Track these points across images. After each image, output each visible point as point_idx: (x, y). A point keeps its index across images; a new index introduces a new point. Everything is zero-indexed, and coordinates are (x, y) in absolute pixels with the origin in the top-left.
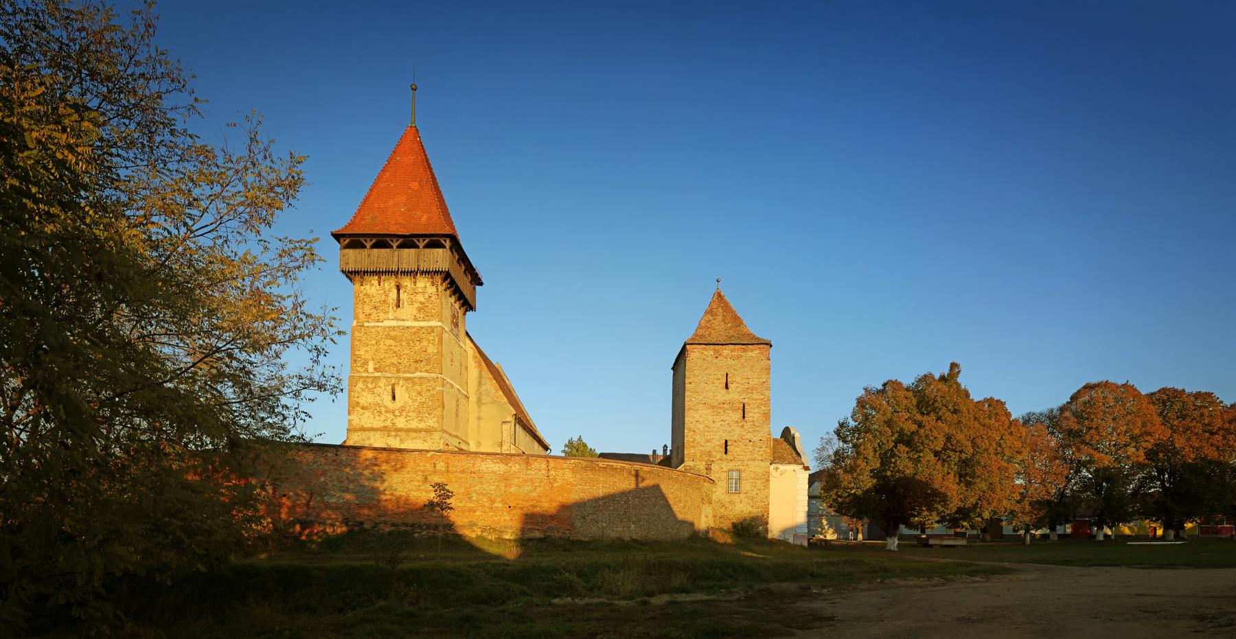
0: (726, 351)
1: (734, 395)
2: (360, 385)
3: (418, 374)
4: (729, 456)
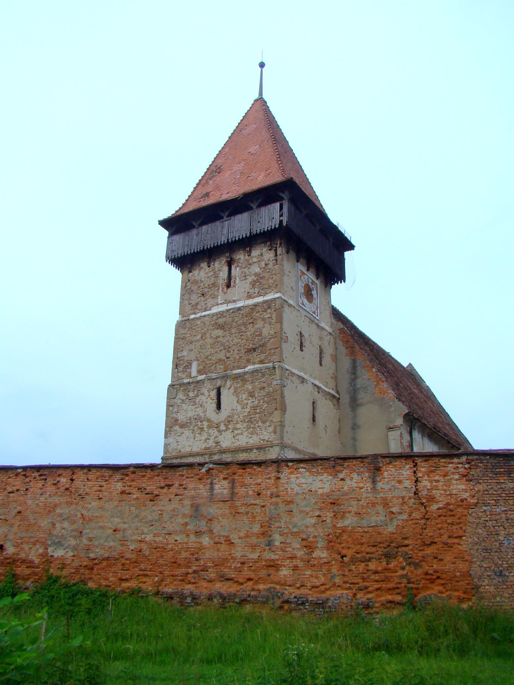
2: (181, 396)
3: (250, 368)
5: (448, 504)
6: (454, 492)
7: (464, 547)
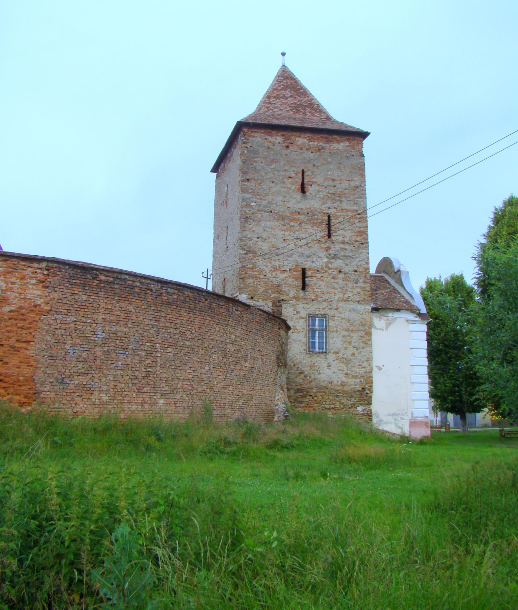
0: (301, 140)
1: (314, 202)
4: (310, 294)
5: (21, 308)
6: (29, 296)
7: (31, 353)
